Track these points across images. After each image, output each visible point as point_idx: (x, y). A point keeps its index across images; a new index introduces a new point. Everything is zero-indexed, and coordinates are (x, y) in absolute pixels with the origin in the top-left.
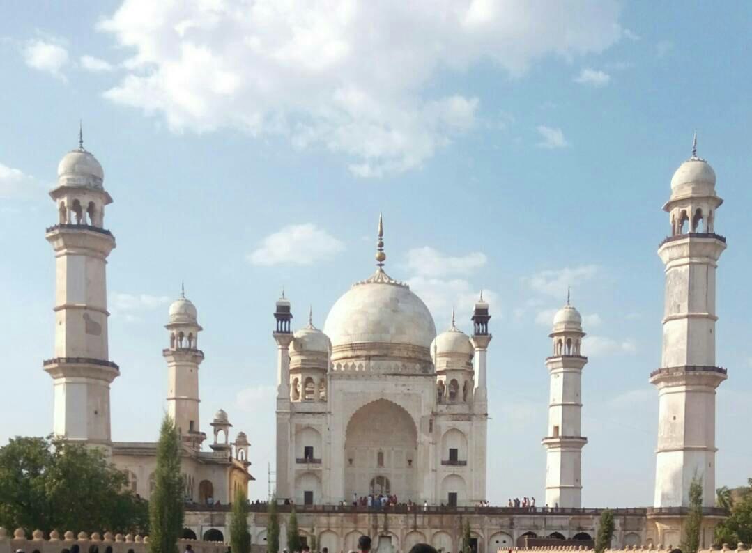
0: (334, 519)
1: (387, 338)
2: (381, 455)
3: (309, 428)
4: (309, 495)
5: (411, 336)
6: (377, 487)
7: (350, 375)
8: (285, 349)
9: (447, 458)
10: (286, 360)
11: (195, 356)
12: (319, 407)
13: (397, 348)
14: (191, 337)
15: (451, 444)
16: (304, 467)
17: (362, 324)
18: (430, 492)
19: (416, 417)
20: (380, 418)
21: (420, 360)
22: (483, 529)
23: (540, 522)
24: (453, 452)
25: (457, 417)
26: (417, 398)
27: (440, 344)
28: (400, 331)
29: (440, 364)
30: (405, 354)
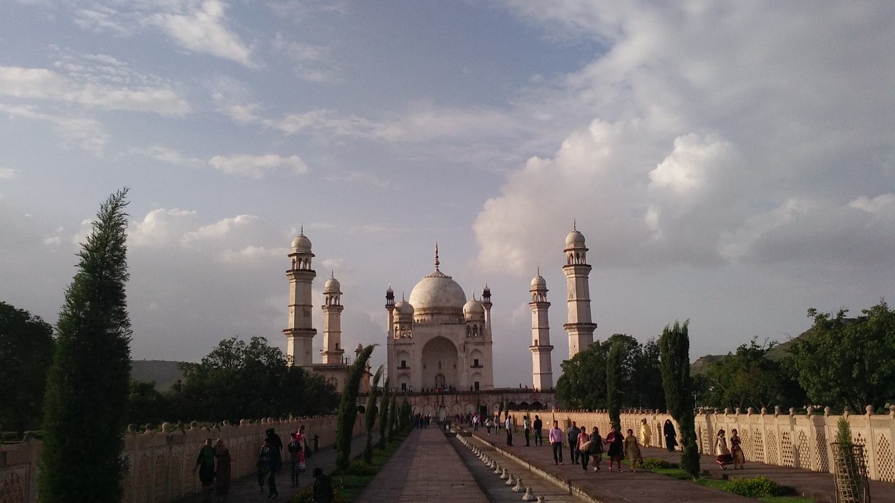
0: (417, 399)
1: (441, 305)
2: (440, 364)
3: (404, 351)
4: (404, 386)
5: (453, 303)
6: (439, 378)
7: (423, 324)
8: (391, 313)
9: (473, 364)
10: (392, 318)
11: (339, 308)
12: (408, 341)
13: (446, 305)
14: (337, 298)
15: (476, 356)
16: (401, 371)
17: (429, 298)
18: (464, 381)
19: (457, 344)
20: (439, 347)
21: (458, 312)
22: (491, 402)
23: (516, 396)
24: (476, 361)
25: (477, 344)
26: (458, 335)
27: (467, 307)
28: (447, 301)
29: (467, 316)
30: (450, 312)
